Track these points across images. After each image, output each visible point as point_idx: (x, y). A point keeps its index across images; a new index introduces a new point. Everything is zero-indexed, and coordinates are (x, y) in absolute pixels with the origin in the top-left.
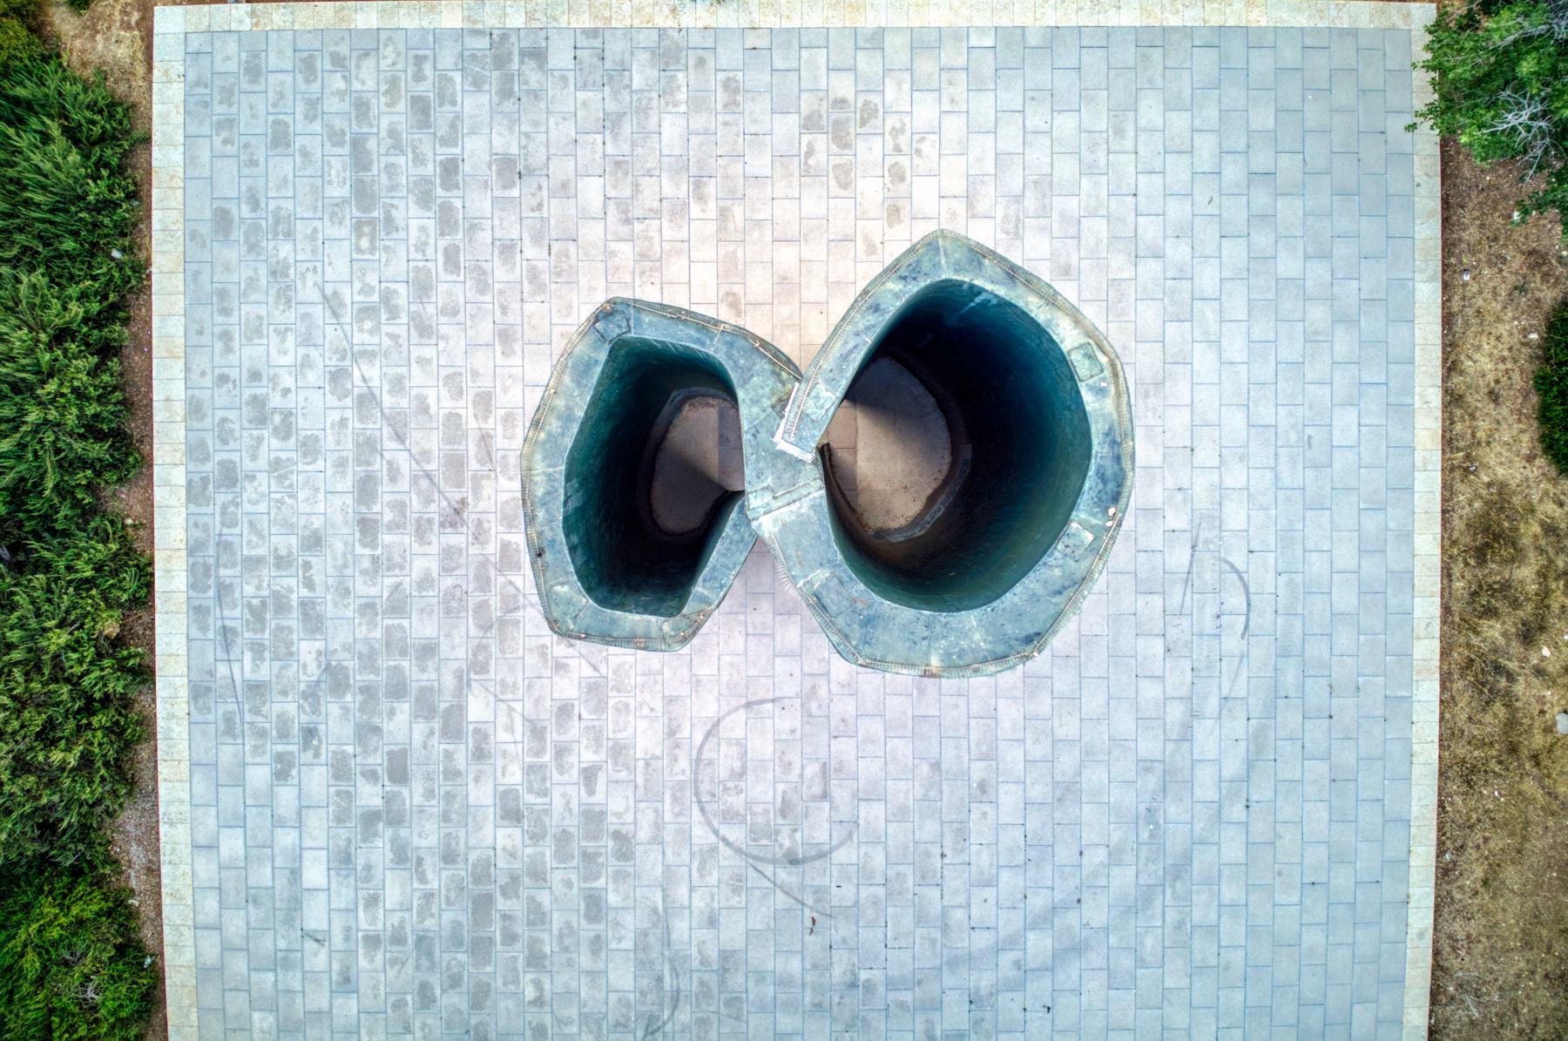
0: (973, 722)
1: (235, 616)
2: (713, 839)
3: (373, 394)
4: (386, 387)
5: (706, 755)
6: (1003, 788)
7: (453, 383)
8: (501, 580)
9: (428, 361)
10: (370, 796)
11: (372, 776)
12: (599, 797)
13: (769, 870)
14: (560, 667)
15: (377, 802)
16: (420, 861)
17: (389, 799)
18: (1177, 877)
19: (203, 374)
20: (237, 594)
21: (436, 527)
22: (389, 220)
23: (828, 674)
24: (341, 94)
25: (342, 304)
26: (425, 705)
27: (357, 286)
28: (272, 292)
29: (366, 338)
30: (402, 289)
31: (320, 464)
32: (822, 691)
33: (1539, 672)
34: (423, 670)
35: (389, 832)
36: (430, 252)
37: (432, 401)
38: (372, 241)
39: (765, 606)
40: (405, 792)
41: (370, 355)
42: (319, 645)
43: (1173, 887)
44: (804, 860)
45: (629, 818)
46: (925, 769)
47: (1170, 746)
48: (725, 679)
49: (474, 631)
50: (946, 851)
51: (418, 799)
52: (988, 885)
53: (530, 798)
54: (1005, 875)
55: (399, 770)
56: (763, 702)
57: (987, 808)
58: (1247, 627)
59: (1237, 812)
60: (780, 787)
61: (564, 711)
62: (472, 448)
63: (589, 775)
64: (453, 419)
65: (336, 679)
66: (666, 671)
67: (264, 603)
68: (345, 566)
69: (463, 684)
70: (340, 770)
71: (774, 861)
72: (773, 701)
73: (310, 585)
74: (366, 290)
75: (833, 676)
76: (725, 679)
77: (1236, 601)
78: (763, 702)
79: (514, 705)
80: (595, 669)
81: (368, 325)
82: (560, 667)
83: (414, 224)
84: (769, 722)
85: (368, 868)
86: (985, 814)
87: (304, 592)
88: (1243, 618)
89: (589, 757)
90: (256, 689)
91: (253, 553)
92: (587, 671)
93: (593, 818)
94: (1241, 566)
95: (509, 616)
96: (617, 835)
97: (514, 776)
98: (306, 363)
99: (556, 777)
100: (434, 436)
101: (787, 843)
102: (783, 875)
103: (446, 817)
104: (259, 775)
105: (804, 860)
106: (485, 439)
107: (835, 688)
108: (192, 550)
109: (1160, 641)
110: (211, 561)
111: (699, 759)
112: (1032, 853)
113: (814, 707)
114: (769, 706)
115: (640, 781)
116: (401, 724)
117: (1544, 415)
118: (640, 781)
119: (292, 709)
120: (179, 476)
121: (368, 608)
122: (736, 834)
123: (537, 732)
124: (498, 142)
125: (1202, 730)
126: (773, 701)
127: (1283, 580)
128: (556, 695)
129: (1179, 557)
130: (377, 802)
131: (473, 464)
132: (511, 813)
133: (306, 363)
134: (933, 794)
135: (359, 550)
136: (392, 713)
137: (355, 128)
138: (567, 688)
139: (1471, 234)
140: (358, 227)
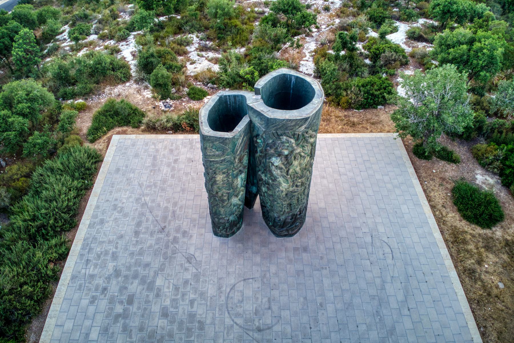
0: (316, 285)
1: (91, 256)
2: (232, 323)
3: (146, 203)
4: (150, 201)
5: (231, 295)
6: (328, 305)
7: (168, 201)
8: (172, 246)
9: (162, 196)
10: (119, 309)
11: (121, 302)
12: (195, 309)
13: (251, 333)
14: (186, 269)
15: (121, 311)
16: (131, 330)
17: (125, 310)
18: (392, 334)
19: (102, 200)
20: (94, 251)
21: (156, 233)
22: (159, 170)
23: (269, 271)
24: (153, 149)
25: (143, 185)
26: (143, 281)
27: (148, 182)
28: (126, 183)
29: (148, 191)
30: (159, 182)
31: (128, 219)
32: (268, 275)
33: (487, 272)
34: (144, 270)
35: (123, 321)
36: (168, 175)
37: (161, 204)
38: (154, 173)
39: (250, 251)
40: (131, 308)
41: (147, 195)
42: (115, 264)
43: (391, 338)
44: (263, 330)
45: (204, 316)
46: (302, 299)
47: (379, 291)
48: (237, 272)
49: (162, 260)
50: (311, 326)
51: (135, 310)
52: (327, 338)
53: (172, 309)
54: (333, 334)
55: (130, 301)
56: (249, 279)
57: (323, 311)
58: (393, 257)
59: (406, 312)
60: (255, 306)
61: (186, 282)
62: (170, 214)
63: (192, 302)
64: (166, 208)
65: (117, 273)
66: (219, 270)
67: (101, 253)
68: (128, 243)
69: (156, 274)
70: (112, 301)
71: (253, 330)
72: (252, 279)
73: (116, 248)
74: (150, 182)
75: (271, 270)
76: (237, 272)
77: (387, 250)
78: (249, 279)
79: (171, 280)
80: (197, 270)
81: (149, 189)
82: (186, 269)
83: (165, 171)
84: (251, 285)
85: (113, 333)
86: (323, 314)
87: (114, 250)
88: (391, 255)
89: (192, 296)
90: (92, 276)
91: (103, 240)
92: (194, 271)
93: (192, 316)
94: (387, 241)
95: (173, 256)
96: (199, 322)
97: (168, 302)
98: (131, 197)
99: (181, 303)
100: (160, 212)
101: (257, 324)
102: (256, 335)
103: (143, 316)
104: (85, 302)
105: (263, 330)
106: (174, 212)
107: (272, 275)
108: (84, 240)
109: (368, 261)
110: (90, 242)
111: (228, 297)
112: (341, 327)
113: (265, 280)
114: (251, 280)
115: (208, 303)
116: (134, 287)
117: (460, 210)
118: (208, 303)
119: (101, 282)
120: (88, 222)
121: (132, 254)
122: (240, 321)
123: (177, 289)
124: (188, 156)
125: (388, 286)
126: (252, 279)
127: (399, 245)
128: (184, 278)
129: (368, 239)
130: (121, 311)
131: (170, 218)
132: (165, 314)
133: (131, 197)
134: (305, 307)
135: (133, 239)
136: (132, 283)
137: (155, 154)
138: (188, 276)
139: (424, 174)
140: (151, 171)
